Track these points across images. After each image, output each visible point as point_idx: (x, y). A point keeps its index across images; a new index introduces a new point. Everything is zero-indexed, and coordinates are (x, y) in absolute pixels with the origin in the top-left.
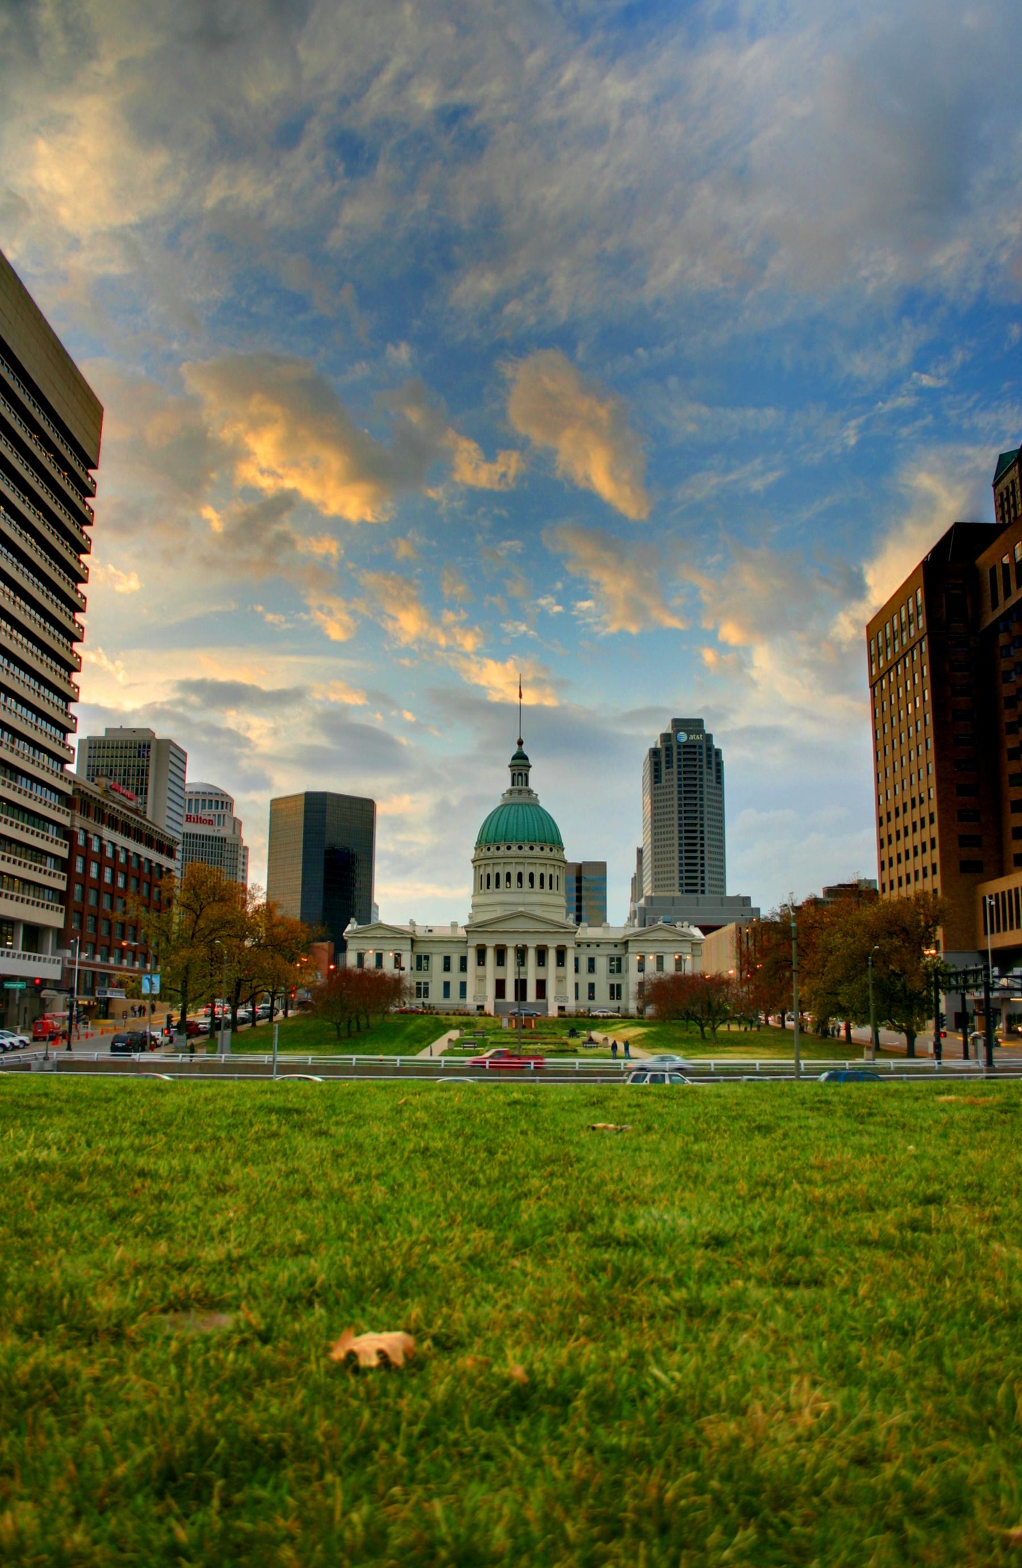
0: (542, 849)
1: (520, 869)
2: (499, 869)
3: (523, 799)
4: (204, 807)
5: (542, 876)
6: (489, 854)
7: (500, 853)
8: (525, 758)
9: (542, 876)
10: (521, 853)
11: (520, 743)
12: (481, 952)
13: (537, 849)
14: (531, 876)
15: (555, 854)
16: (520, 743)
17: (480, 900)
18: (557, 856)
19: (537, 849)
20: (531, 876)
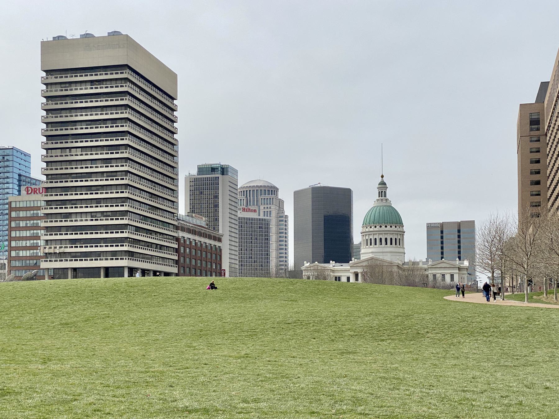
0: (391, 227)
2: (371, 237)
3: (384, 203)
4: (261, 194)
5: (391, 239)
6: (367, 230)
7: (371, 230)
8: (385, 184)
9: (391, 239)
10: (380, 229)
13: (388, 227)
14: (386, 239)
16: (382, 177)
18: (399, 230)
19: (388, 227)
20: (386, 239)
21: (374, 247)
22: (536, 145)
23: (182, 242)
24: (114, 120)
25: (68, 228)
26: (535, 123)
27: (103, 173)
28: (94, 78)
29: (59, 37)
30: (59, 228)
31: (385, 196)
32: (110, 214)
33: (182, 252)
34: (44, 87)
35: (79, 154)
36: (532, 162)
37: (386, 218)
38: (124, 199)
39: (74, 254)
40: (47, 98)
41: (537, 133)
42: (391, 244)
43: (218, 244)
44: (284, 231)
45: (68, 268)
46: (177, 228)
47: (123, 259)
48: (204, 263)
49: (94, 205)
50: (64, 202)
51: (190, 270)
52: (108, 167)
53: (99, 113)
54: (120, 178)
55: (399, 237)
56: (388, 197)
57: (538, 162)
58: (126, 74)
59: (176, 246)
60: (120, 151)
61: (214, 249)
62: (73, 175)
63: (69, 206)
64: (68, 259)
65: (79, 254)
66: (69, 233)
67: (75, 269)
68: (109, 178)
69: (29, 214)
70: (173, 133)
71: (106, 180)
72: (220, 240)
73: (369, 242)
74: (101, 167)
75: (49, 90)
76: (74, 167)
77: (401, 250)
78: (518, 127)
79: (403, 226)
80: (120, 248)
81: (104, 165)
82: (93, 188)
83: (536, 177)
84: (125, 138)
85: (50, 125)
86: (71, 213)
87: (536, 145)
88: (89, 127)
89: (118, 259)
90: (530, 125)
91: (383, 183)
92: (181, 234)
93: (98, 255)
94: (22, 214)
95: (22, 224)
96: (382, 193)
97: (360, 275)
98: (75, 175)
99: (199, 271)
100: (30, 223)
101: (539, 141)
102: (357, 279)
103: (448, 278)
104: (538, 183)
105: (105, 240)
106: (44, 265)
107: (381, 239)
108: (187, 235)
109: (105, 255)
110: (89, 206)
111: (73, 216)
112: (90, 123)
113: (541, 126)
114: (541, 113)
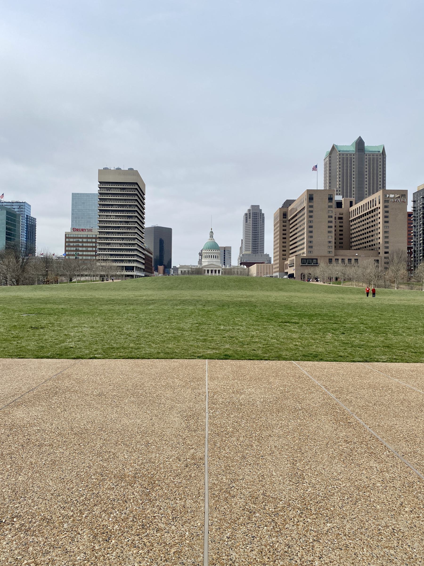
12: (208, 271)
27: (125, 227)
50: (107, 238)
69: (75, 240)
72: (152, 254)
86: (110, 243)
94: (71, 240)
95: (71, 244)
100: (75, 244)
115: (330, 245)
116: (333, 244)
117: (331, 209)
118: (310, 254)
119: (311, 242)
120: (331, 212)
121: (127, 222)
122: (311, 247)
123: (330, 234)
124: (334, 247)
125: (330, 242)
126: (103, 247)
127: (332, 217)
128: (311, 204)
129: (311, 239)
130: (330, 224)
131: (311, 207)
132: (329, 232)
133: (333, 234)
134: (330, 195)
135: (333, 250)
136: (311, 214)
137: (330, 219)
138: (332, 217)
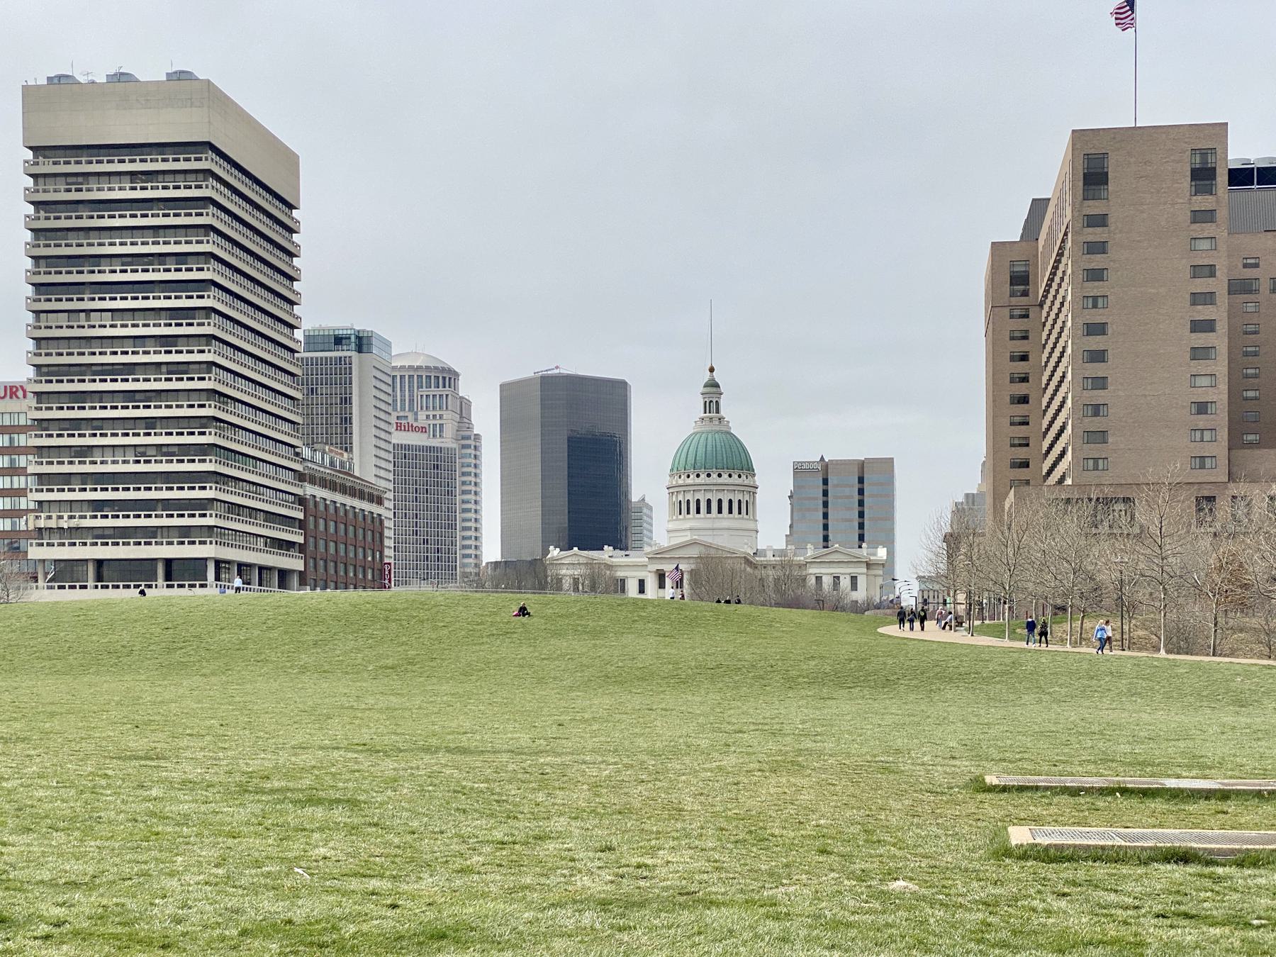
1: (709, 496)
2: (689, 496)
5: (730, 501)
6: (681, 482)
7: (689, 481)
9: (730, 501)
10: (708, 480)
11: (712, 370)
13: (725, 476)
14: (720, 501)
15: (744, 480)
16: (712, 370)
17: (671, 526)
18: (746, 482)
19: (725, 476)
20: (720, 501)
21: (694, 518)
22: (1021, 324)
23: (311, 503)
24: (181, 257)
25: (85, 477)
26: (1020, 280)
28: (138, 167)
29: (60, 77)
30: (66, 478)
31: (718, 412)
32: (175, 449)
33: (312, 526)
34: (30, 182)
35: (108, 323)
36: (1012, 359)
37: (719, 458)
38: (204, 421)
39: (100, 532)
40: (37, 204)
41: (1024, 300)
42: (730, 512)
43: (376, 509)
44: (472, 470)
45: (87, 560)
46: (301, 477)
47: (204, 543)
48: (342, 547)
49: (142, 432)
51: (336, 567)
52: (170, 352)
53: (150, 240)
54: (196, 376)
55: (747, 497)
56: (723, 413)
57: (1024, 358)
58: (208, 162)
59: (301, 516)
60: (195, 322)
61: (351, 515)
62: (94, 368)
63: (87, 432)
64: (88, 541)
65: (111, 532)
66: (88, 487)
67: (100, 563)
68: (174, 377)
70: (292, 279)
71: (166, 380)
72: (380, 501)
73: (684, 508)
74: (155, 352)
75: (41, 188)
76: (97, 351)
77: (751, 525)
78: (987, 286)
79: (754, 475)
80: (198, 521)
81: (163, 349)
82: (138, 396)
83: (1021, 389)
84: (206, 294)
85: (42, 262)
87: (1021, 324)
88: (129, 268)
89: (194, 543)
90: (1011, 284)
91: (713, 384)
92: (310, 490)
93: (150, 534)
96: (712, 406)
97: (686, 577)
98: (99, 368)
99: (322, 563)
101: (1027, 316)
102: (662, 585)
103: (845, 583)
104: (1024, 400)
105: (167, 504)
106: (35, 553)
107: (709, 501)
108: (320, 493)
109: (165, 534)
110: (131, 432)
111: (97, 452)
112: (129, 259)
113: (1031, 287)
114: (1031, 261)
115: (1202, 421)
116: (1220, 418)
117: (1209, 230)
118: (1091, 477)
119: (1096, 410)
120: (1205, 245)
121: (167, 341)
122: (1099, 437)
123: (1201, 367)
124: (1223, 434)
125: (1202, 408)
126: (55, 469)
127: (1211, 271)
128: (1095, 208)
129: (1099, 396)
130: (1204, 313)
131: (1099, 221)
132: (1199, 353)
133: (1220, 366)
134: (1204, 153)
135: (1219, 448)
136: (1097, 261)
137: (1202, 285)
138: (1211, 271)
